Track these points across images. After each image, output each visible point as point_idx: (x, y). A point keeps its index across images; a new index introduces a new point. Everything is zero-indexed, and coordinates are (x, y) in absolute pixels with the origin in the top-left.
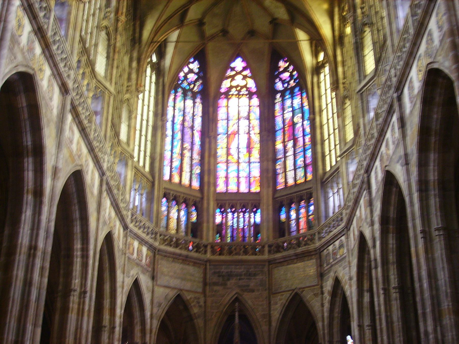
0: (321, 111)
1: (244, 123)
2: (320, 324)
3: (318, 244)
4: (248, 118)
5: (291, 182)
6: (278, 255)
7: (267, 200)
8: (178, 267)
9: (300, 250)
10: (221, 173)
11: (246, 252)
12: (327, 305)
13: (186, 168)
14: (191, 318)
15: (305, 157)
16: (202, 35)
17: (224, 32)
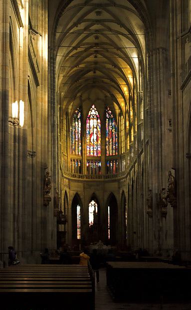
0: (121, 130)
1: (95, 130)
2: (118, 203)
3: (119, 178)
4: (97, 128)
5: (111, 154)
6: (106, 180)
7: (103, 158)
8: (76, 184)
9: (114, 179)
10: (88, 149)
11: (96, 178)
12: (120, 197)
13: (77, 149)
14: (80, 199)
15: (115, 146)
16: (81, 99)
17: (89, 99)
